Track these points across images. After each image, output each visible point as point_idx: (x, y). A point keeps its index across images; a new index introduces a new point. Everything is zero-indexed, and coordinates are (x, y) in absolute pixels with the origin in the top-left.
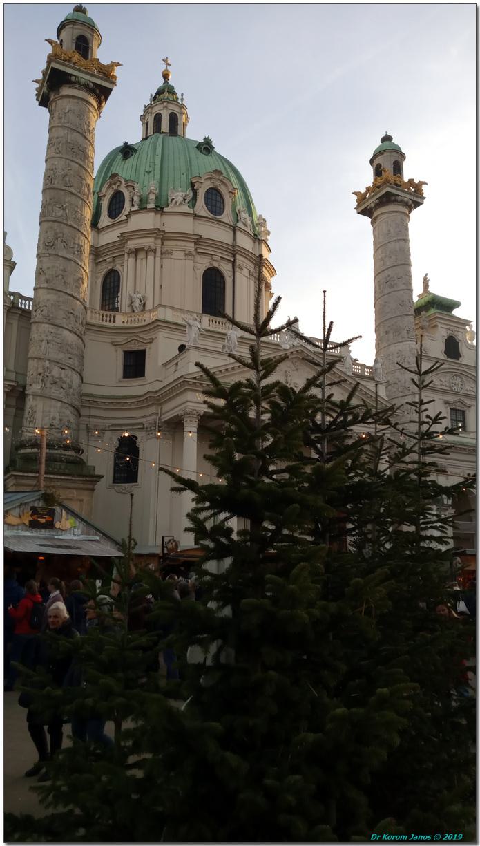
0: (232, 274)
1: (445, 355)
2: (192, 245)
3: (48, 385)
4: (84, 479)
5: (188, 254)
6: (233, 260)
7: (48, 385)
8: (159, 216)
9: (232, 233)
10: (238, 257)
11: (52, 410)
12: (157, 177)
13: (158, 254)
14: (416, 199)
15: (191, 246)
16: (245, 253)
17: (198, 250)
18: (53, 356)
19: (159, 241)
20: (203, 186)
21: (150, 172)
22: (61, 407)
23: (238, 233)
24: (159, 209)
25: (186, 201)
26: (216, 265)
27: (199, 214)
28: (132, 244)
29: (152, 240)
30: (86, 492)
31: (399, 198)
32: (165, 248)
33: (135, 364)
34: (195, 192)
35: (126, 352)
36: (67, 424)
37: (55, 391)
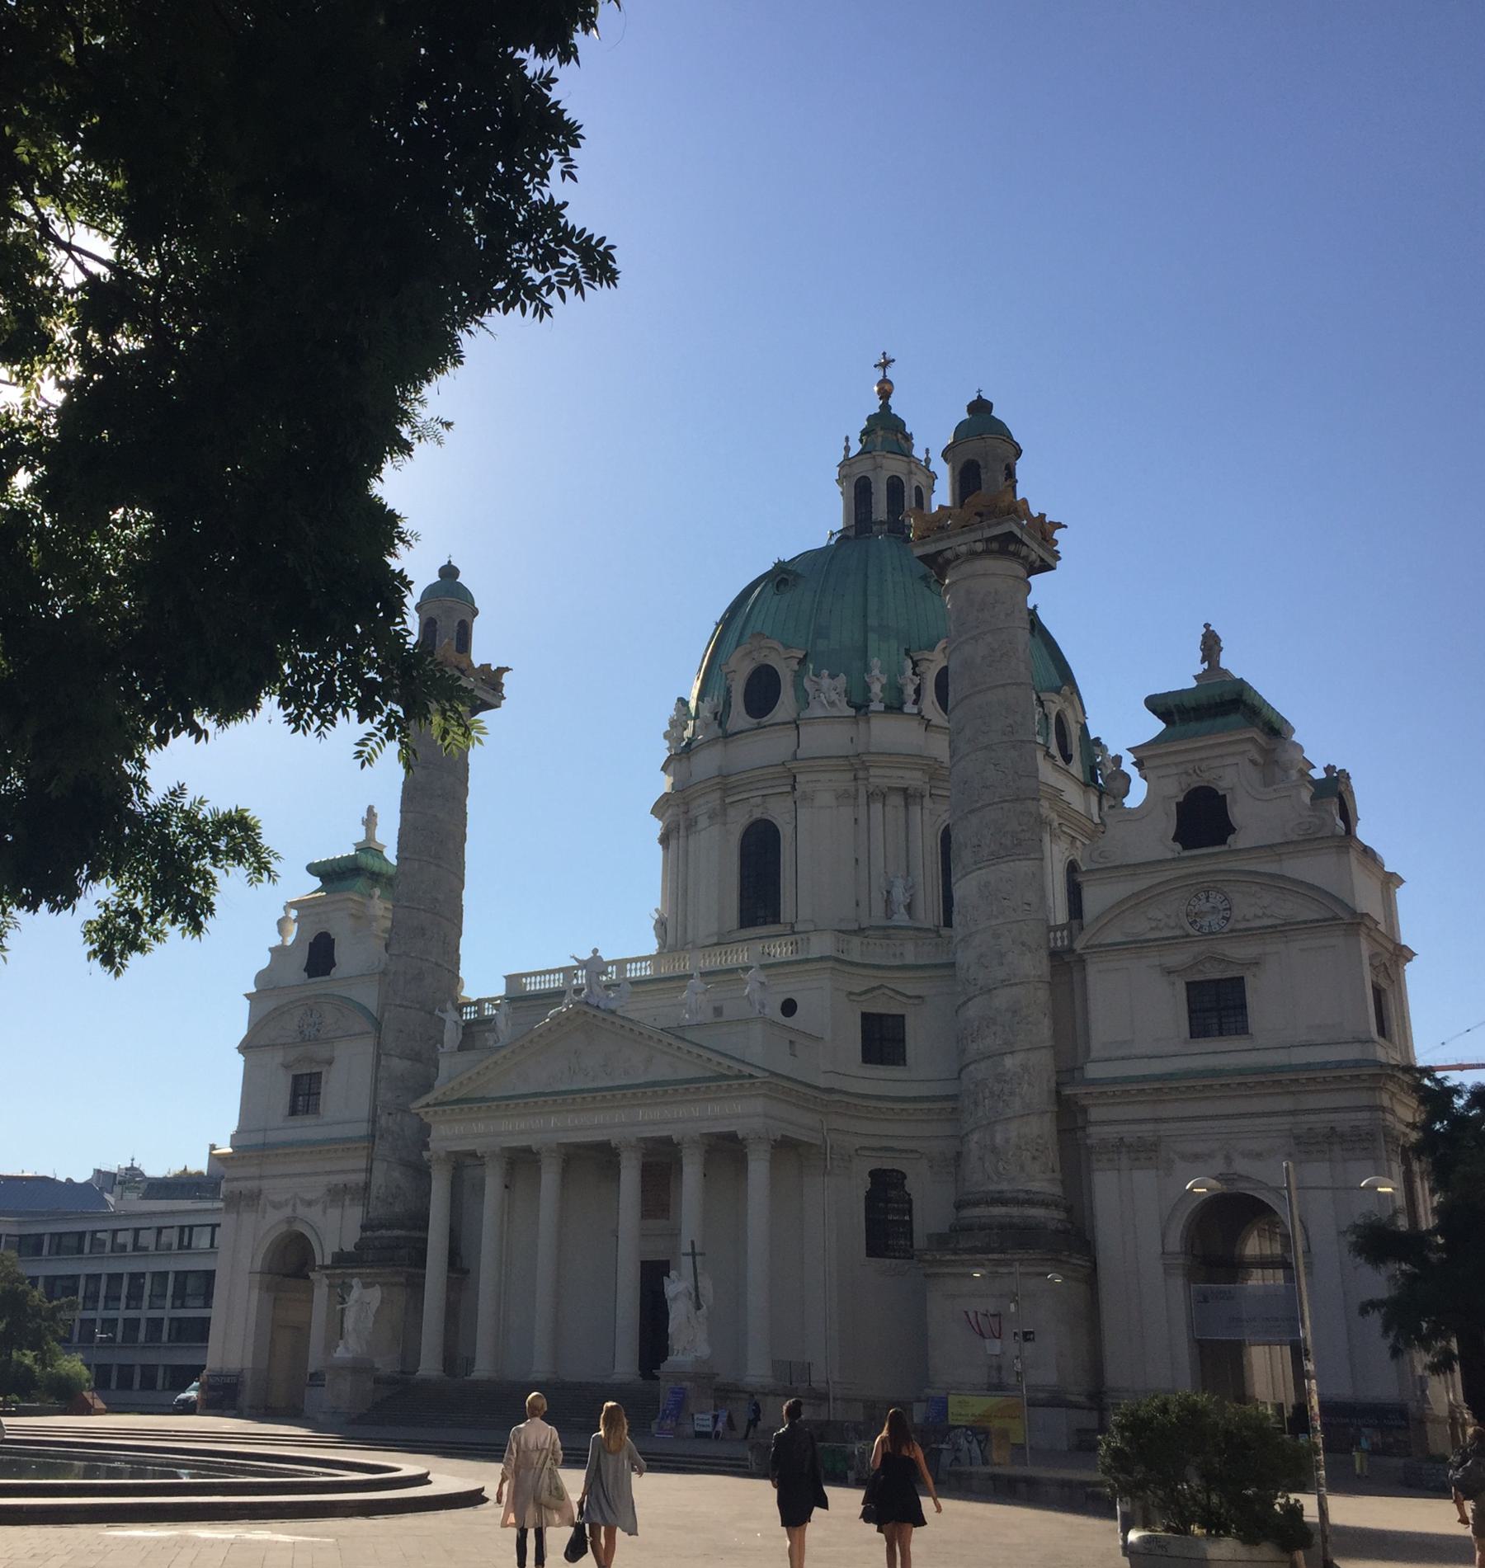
1: (1178, 846)
2: (717, 795)
6: (788, 789)
14: (988, 533)
17: (728, 800)
26: (757, 814)
31: (949, 555)
34: (728, 691)
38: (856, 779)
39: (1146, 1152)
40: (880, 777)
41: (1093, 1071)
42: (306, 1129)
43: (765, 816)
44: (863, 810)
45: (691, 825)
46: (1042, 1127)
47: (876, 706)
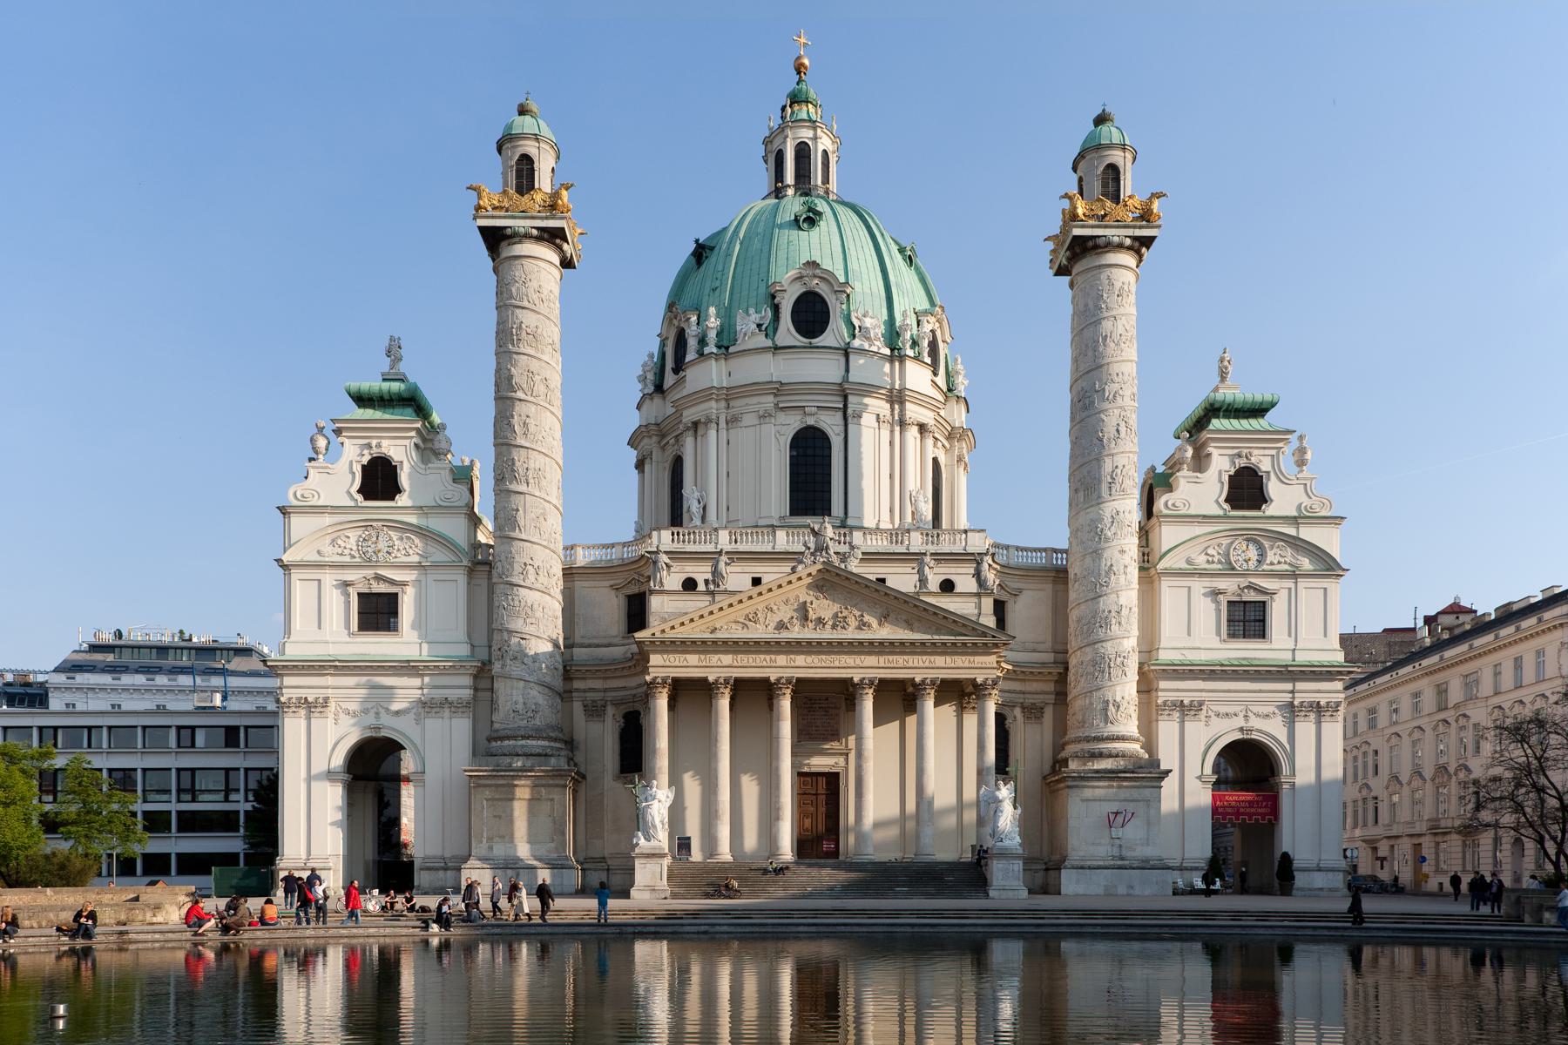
0: (842, 428)
2: (771, 398)
5: (764, 417)
9: (843, 360)
10: (851, 398)
13: (723, 424)
15: (769, 401)
16: (868, 389)
19: (723, 404)
20: (786, 295)
21: (714, 290)
23: (852, 357)
26: (811, 421)
28: (689, 415)
29: (713, 404)
32: (732, 411)
33: (637, 613)
34: (776, 309)
35: (630, 598)
37: (515, 669)
38: (892, 409)
41: (1165, 656)
42: (377, 646)
44: (897, 433)
45: (733, 421)
47: (910, 352)
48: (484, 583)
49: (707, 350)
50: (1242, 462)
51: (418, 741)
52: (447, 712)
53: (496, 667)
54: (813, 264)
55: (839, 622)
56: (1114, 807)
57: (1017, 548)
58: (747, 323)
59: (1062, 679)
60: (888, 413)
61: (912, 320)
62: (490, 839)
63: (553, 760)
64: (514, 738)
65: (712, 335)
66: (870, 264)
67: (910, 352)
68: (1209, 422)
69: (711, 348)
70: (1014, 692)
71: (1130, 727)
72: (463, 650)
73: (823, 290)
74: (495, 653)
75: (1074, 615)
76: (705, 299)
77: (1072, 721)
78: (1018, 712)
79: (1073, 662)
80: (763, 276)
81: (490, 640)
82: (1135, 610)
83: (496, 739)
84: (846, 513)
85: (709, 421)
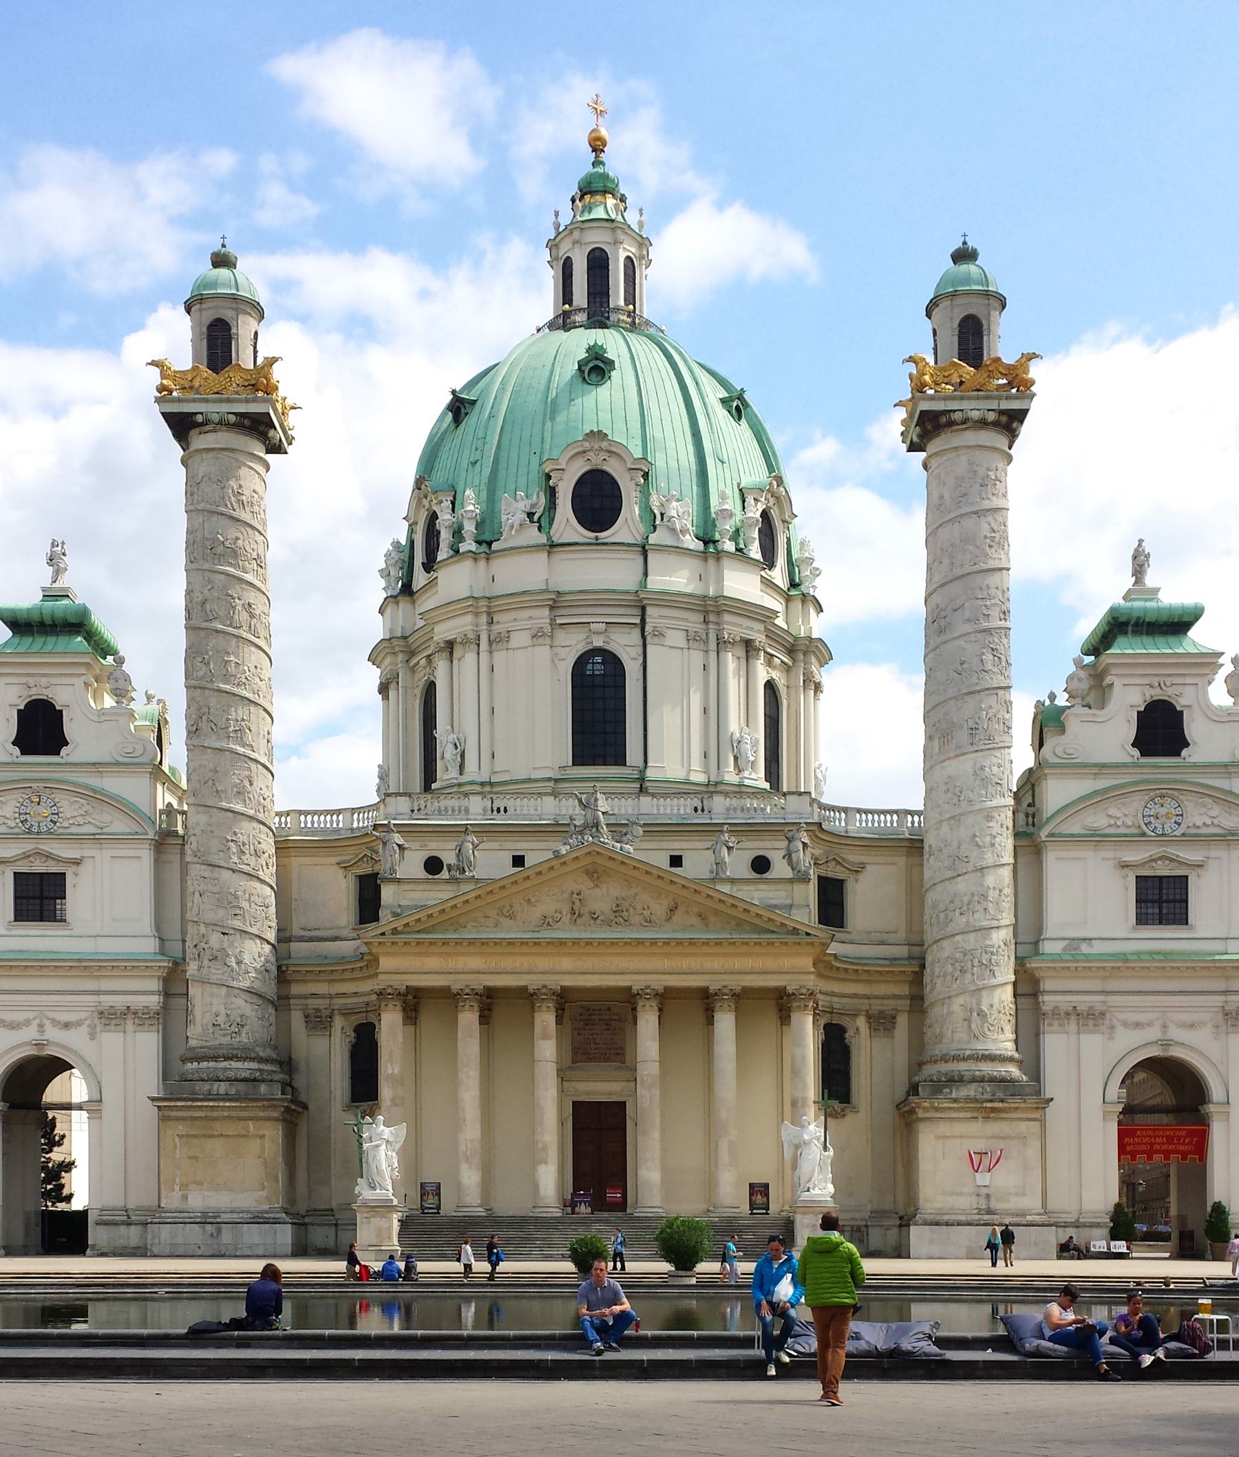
0: (640, 650)
2: (546, 611)
3: (206, 962)
4: (260, 1104)
6: (638, 621)
7: (206, 962)
8: (482, 563)
9: (641, 558)
10: (649, 611)
11: (215, 1000)
12: (487, 472)
16: (670, 600)
18: (209, 916)
19: (484, 619)
20: (566, 476)
22: (228, 995)
24: (484, 548)
25: (536, 517)
26: (598, 642)
27: (561, 541)
29: (469, 619)
30: (268, 1124)
33: (368, 902)
36: (239, 1020)
37: (216, 973)
38: (706, 622)
39: (1090, 1019)
40: (735, 627)
42: (38, 939)
43: (607, 647)
44: (713, 655)
46: (1007, 994)
47: (729, 546)
48: (176, 859)
49: (463, 547)
50: (1157, 694)
51: (91, 1059)
52: (130, 1026)
53: (192, 968)
54: (599, 435)
55: (619, 913)
56: (980, 1145)
57: (859, 811)
58: (513, 510)
59: (917, 978)
60: (700, 627)
61: (733, 504)
62: (184, 1186)
63: (263, 1088)
64: (215, 1058)
65: (469, 527)
66: (677, 424)
67: (729, 546)
68: (1115, 638)
69: (468, 545)
70: (856, 996)
71: (1004, 1043)
72: (149, 946)
73: (613, 468)
74: (191, 952)
75: (931, 897)
76: (463, 474)
77: (929, 1033)
78: (861, 1022)
79: (929, 959)
80: (536, 446)
81: (184, 932)
82: (1009, 891)
83: (192, 1060)
84: (646, 762)
85: (465, 642)
